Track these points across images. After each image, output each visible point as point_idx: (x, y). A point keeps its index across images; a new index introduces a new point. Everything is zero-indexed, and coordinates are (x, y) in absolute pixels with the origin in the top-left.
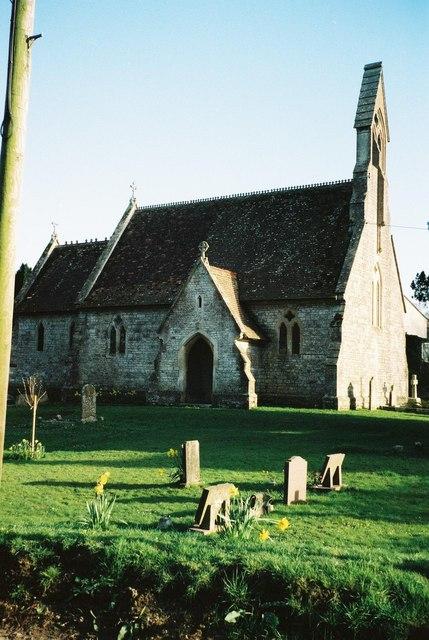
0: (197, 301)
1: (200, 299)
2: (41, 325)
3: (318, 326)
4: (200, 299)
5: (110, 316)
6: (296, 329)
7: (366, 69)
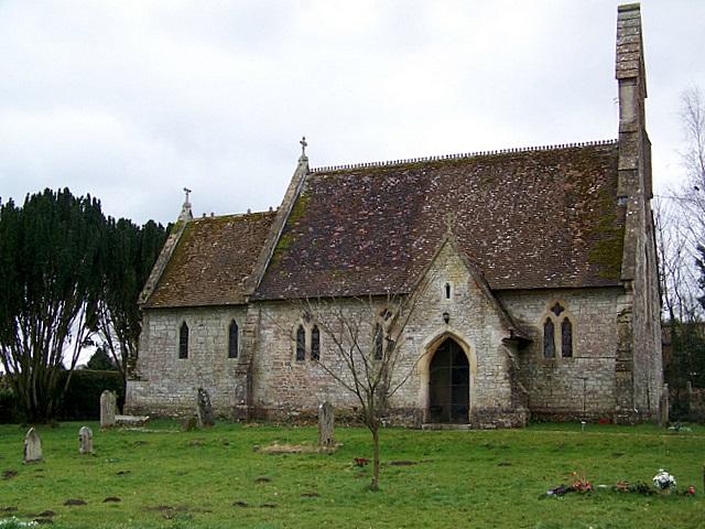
0: (445, 291)
1: (448, 288)
2: (184, 323)
3: (598, 321)
4: (448, 288)
5: (297, 311)
6: (566, 324)
7: (619, 11)
